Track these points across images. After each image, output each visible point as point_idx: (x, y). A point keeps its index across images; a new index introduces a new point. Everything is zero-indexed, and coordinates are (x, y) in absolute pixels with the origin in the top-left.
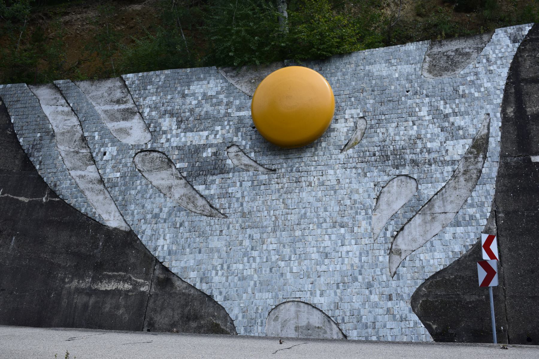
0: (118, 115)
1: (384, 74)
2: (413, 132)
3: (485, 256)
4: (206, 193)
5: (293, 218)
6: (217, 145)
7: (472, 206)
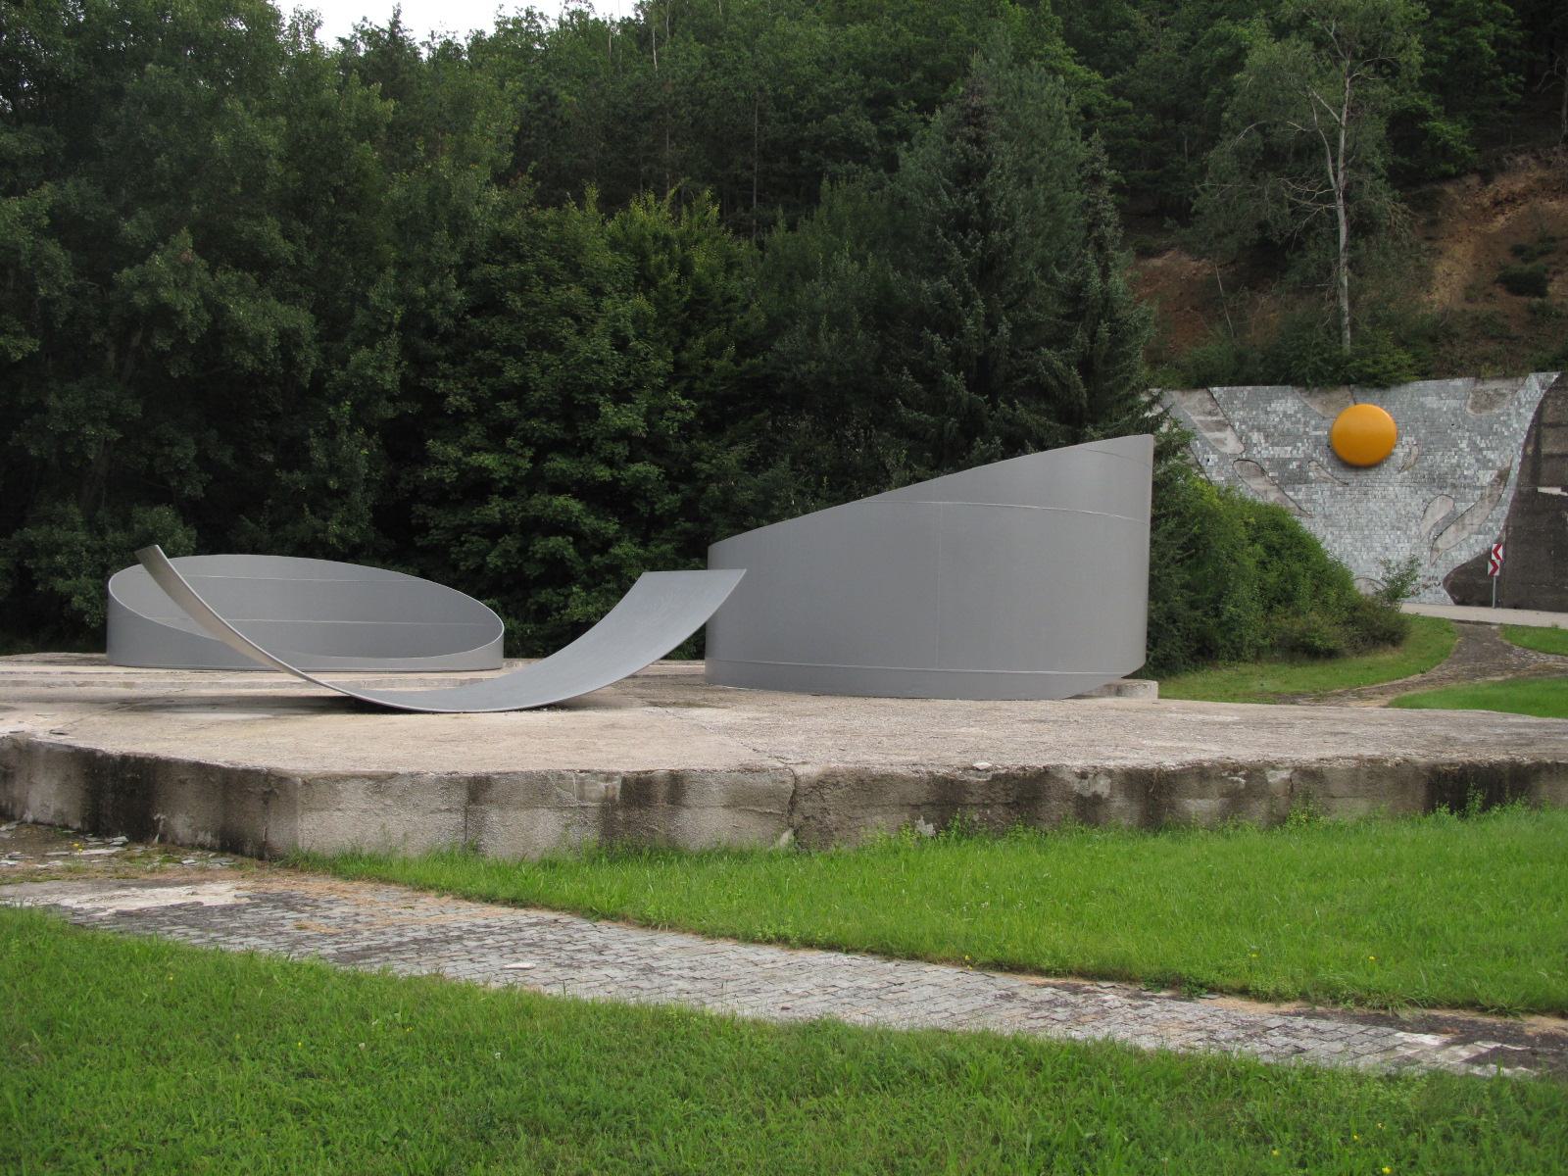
0: (1213, 426)
1: (1435, 406)
2: (1454, 461)
3: (1494, 557)
5: (1363, 521)
7: (1491, 521)
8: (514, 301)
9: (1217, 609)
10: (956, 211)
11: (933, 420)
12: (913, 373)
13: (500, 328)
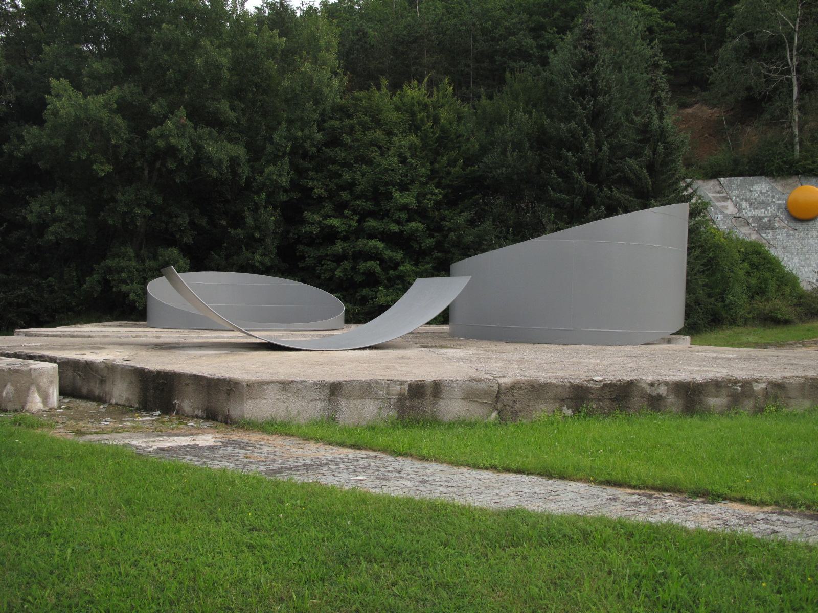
4: (767, 237)
6: (769, 217)
8: (347, 139)
9: (722, 298)
10: (579, 85)
11: (567, 197)
12: (557, 172)
13: (340, 153)
